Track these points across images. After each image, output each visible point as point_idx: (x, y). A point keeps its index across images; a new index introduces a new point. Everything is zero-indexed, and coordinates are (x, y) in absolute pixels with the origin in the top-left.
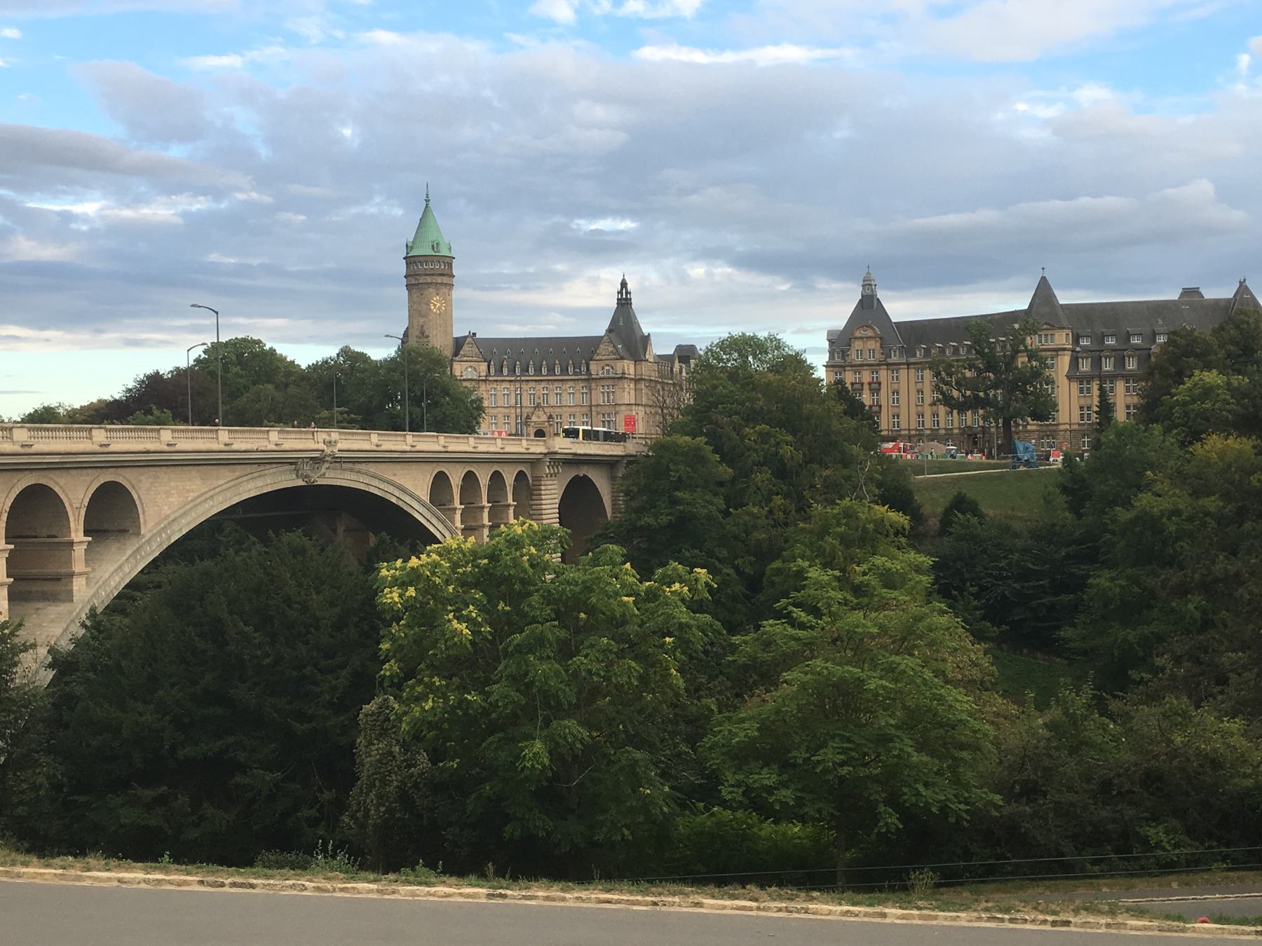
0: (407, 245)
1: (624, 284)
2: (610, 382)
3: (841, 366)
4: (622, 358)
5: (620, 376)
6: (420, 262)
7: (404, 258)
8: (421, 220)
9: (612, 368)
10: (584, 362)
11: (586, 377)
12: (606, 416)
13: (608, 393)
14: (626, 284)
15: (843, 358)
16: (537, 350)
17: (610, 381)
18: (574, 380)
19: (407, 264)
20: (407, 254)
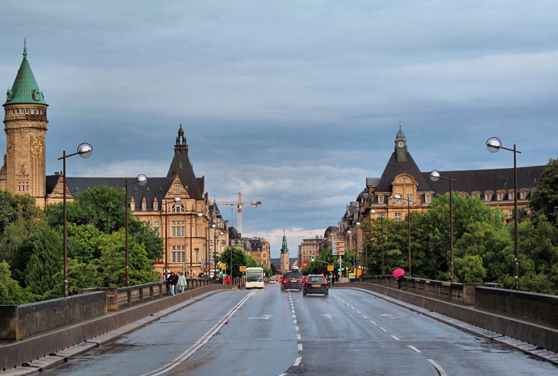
0: (8, 94)
1: (181, 133)
2: (181, 218)
3: (385, 208)
4: (191, 198)
5: (189, 213)
6: (22, 109)
7: (3, 106)
8: (19, 71)
9: (182, 206)
10: (156, 199)
11: (159, 213)
12: (176, 247)
13: (178, 228)
14: (183, 133)
15: (386, 202)
16: (148, 189)
17: (180, 216)
18: (148, 216)
19: (6, 111)
20: (8, 101)
